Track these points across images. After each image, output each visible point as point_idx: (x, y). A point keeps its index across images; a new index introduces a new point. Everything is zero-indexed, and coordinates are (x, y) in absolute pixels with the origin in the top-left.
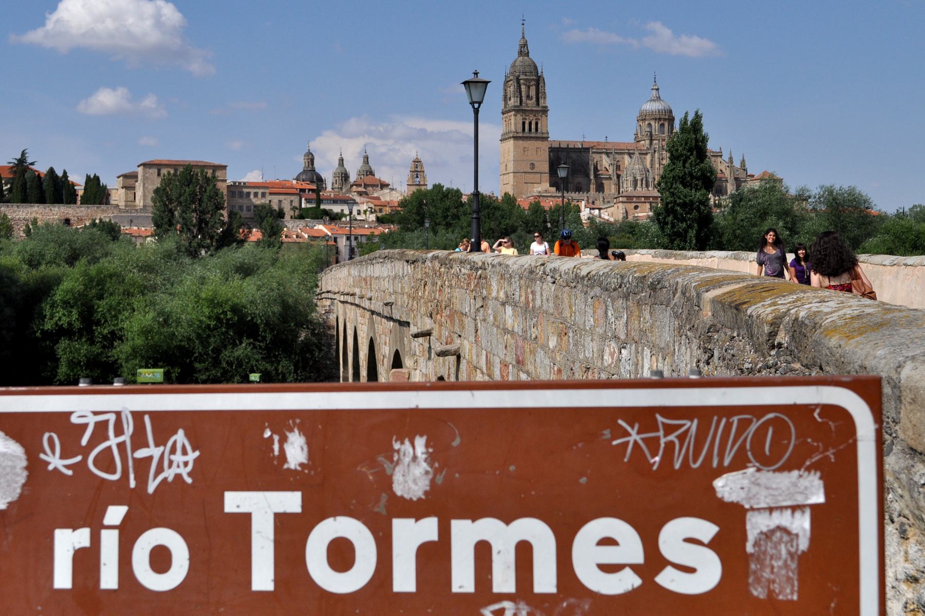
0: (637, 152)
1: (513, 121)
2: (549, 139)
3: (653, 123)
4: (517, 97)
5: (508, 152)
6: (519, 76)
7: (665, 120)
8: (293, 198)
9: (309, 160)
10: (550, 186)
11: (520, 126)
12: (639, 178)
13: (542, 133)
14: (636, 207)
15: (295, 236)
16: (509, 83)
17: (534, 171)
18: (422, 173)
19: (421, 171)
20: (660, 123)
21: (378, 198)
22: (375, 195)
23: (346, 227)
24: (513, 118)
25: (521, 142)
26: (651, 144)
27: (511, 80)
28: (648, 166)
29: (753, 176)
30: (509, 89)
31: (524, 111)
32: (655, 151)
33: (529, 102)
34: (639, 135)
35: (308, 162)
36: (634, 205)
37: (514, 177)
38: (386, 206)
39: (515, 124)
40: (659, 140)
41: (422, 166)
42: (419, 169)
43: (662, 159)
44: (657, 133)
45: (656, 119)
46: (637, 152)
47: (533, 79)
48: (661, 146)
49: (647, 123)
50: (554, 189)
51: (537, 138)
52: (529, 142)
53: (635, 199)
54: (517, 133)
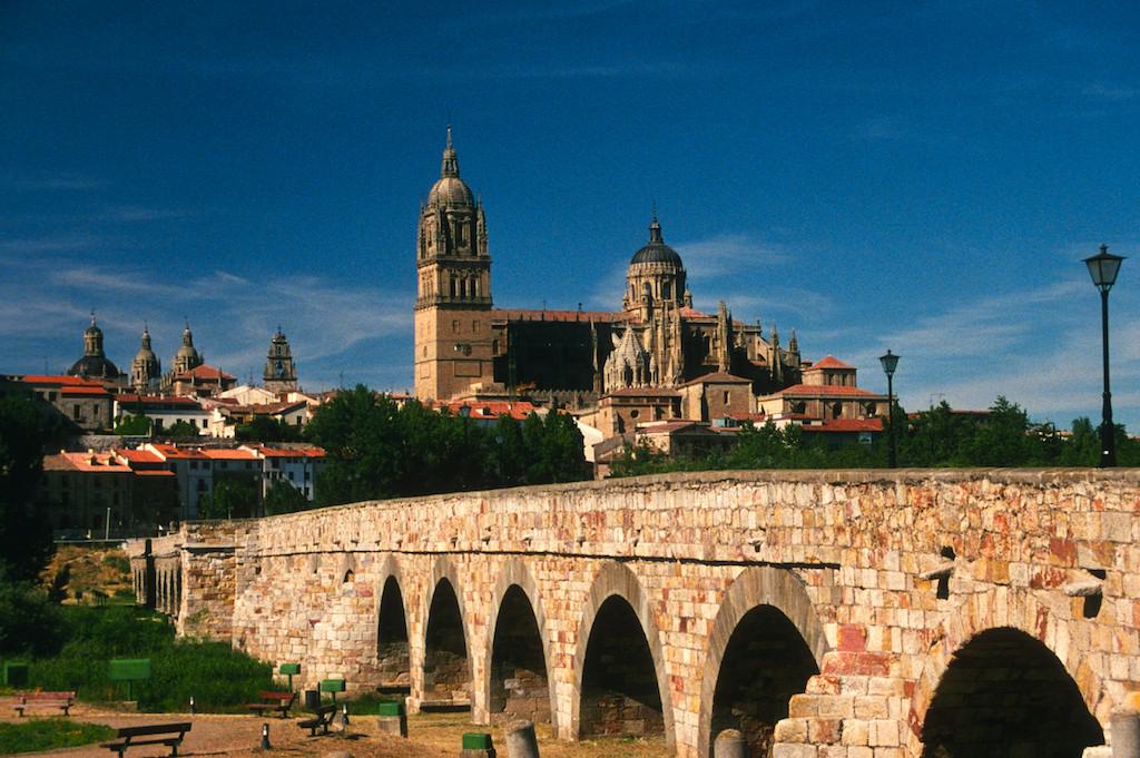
0: (629, 329)
1: (435, 280)
2: (493, 308)
3: (652, 281)
4: (442, 241)
5: (429, 327)
6: (445, 208)
7: (671, 276)
8: (97, 401)
9: (95, 341)
10: (495, 381)
11: (447, 286)
12: (634, 368)
13: (482, 298)
14: (634, 414)
15: (107, 462)
16: (430, 219)
17: (469, 357)
18: (288, 362)
19: (287, 359)
20: (665, 281)
21: (234, 401)
22: (225, 395)
23: (187, 447)
24: (435, 274)
25: (448, 312)
26: (650, 314)
27: (433, 214)
28: (647, 348)
29: (810, 364)
30: (428, 229)
31: (453, 264)
32: (657, 326)
33: (460, 249)
34: (631, 300)
35: (93, 344)
36: (630, 410)
37: (438, 366)
38: (248, 413)
39: (440, 283)
40: (664, 308)
41: (288, 350)
42: (283, 354)
43: (669, 338)
44: (659, 298)
45: (657, 276)
46: (629, 329)
47: (465, 214)
48: (666, 317)
49: (643, 280)
50: (500, 385)
51: (474, 307)
52: (461, 312)
53: (632, 401)
54: (443, 298)
